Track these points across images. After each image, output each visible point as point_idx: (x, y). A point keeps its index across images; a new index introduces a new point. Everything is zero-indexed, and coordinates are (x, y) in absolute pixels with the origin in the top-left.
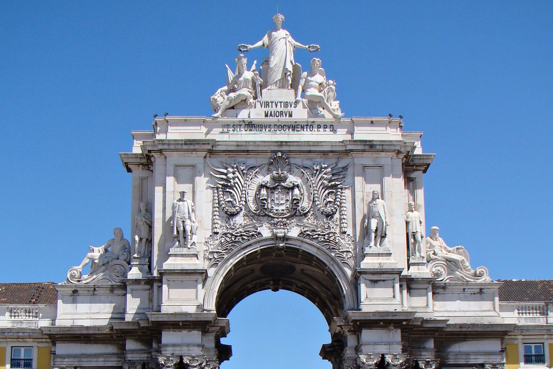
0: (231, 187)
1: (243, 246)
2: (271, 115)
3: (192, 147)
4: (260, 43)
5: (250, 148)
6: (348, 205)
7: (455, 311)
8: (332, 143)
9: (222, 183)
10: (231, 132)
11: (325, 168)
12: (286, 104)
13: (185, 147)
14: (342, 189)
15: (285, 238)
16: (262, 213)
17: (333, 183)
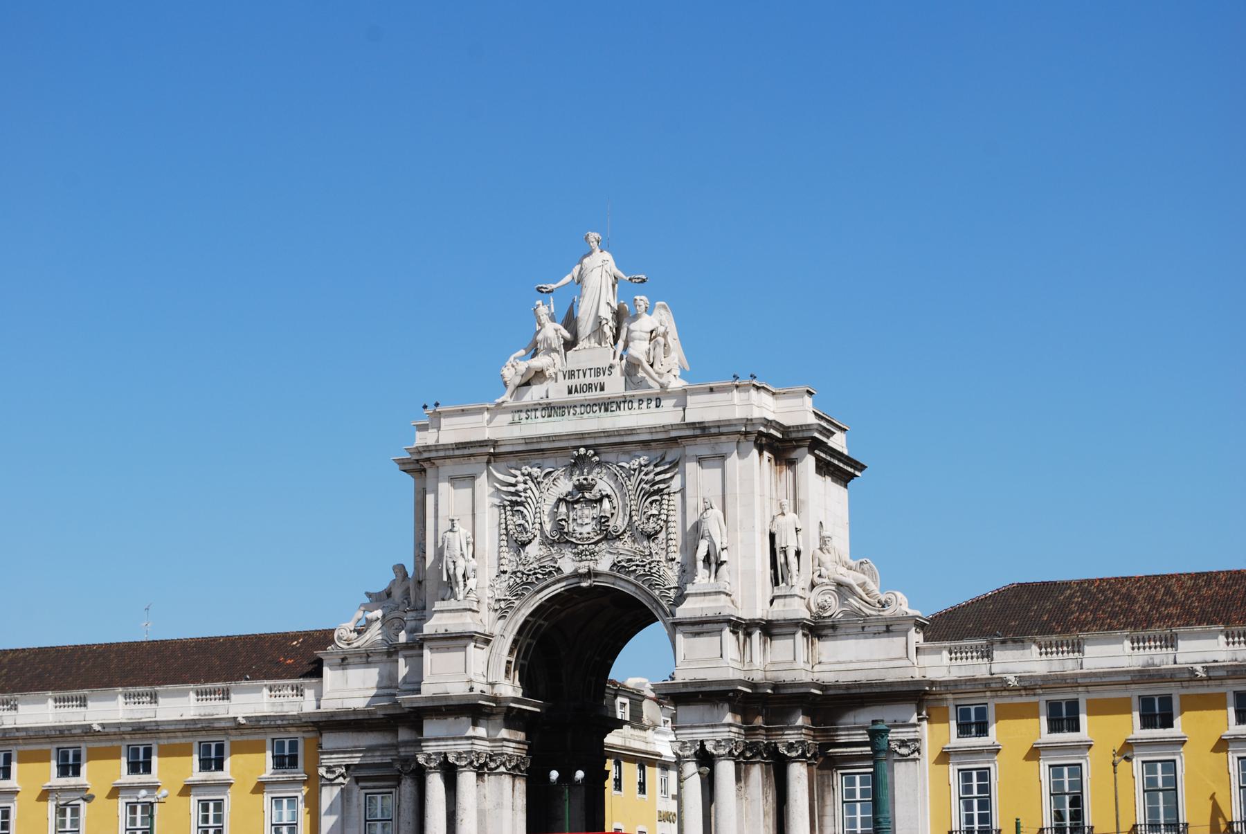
0: (521, 504)
1: (537, 588)
2: (576, 391)
3: (466, 452)
4: (568, 278)
5: (544, 446)
6: (676, 518)
7: (851, 662)
8: (651, 430)
9: (510, 498)
10: (524, 421)
11: (645, 466)
12: (598, 372)
13: (457, 452)
14: (669, 494)
15: (590, 574)
16: (561, 538)
17: (656, 487)
